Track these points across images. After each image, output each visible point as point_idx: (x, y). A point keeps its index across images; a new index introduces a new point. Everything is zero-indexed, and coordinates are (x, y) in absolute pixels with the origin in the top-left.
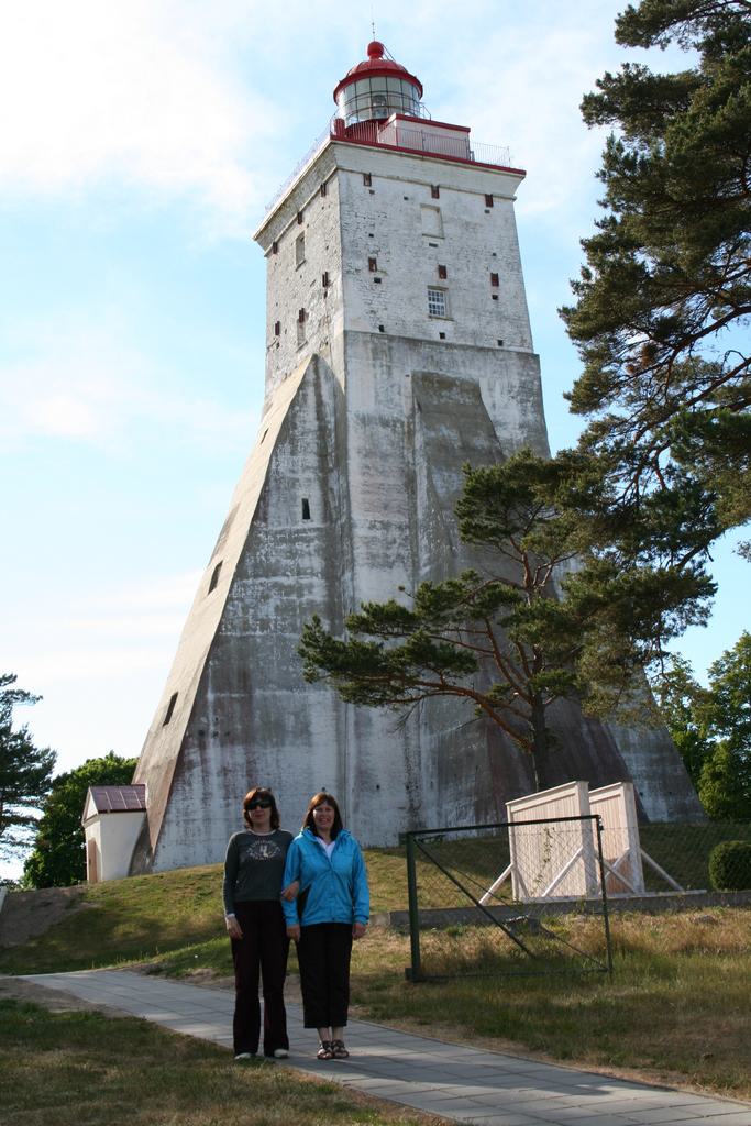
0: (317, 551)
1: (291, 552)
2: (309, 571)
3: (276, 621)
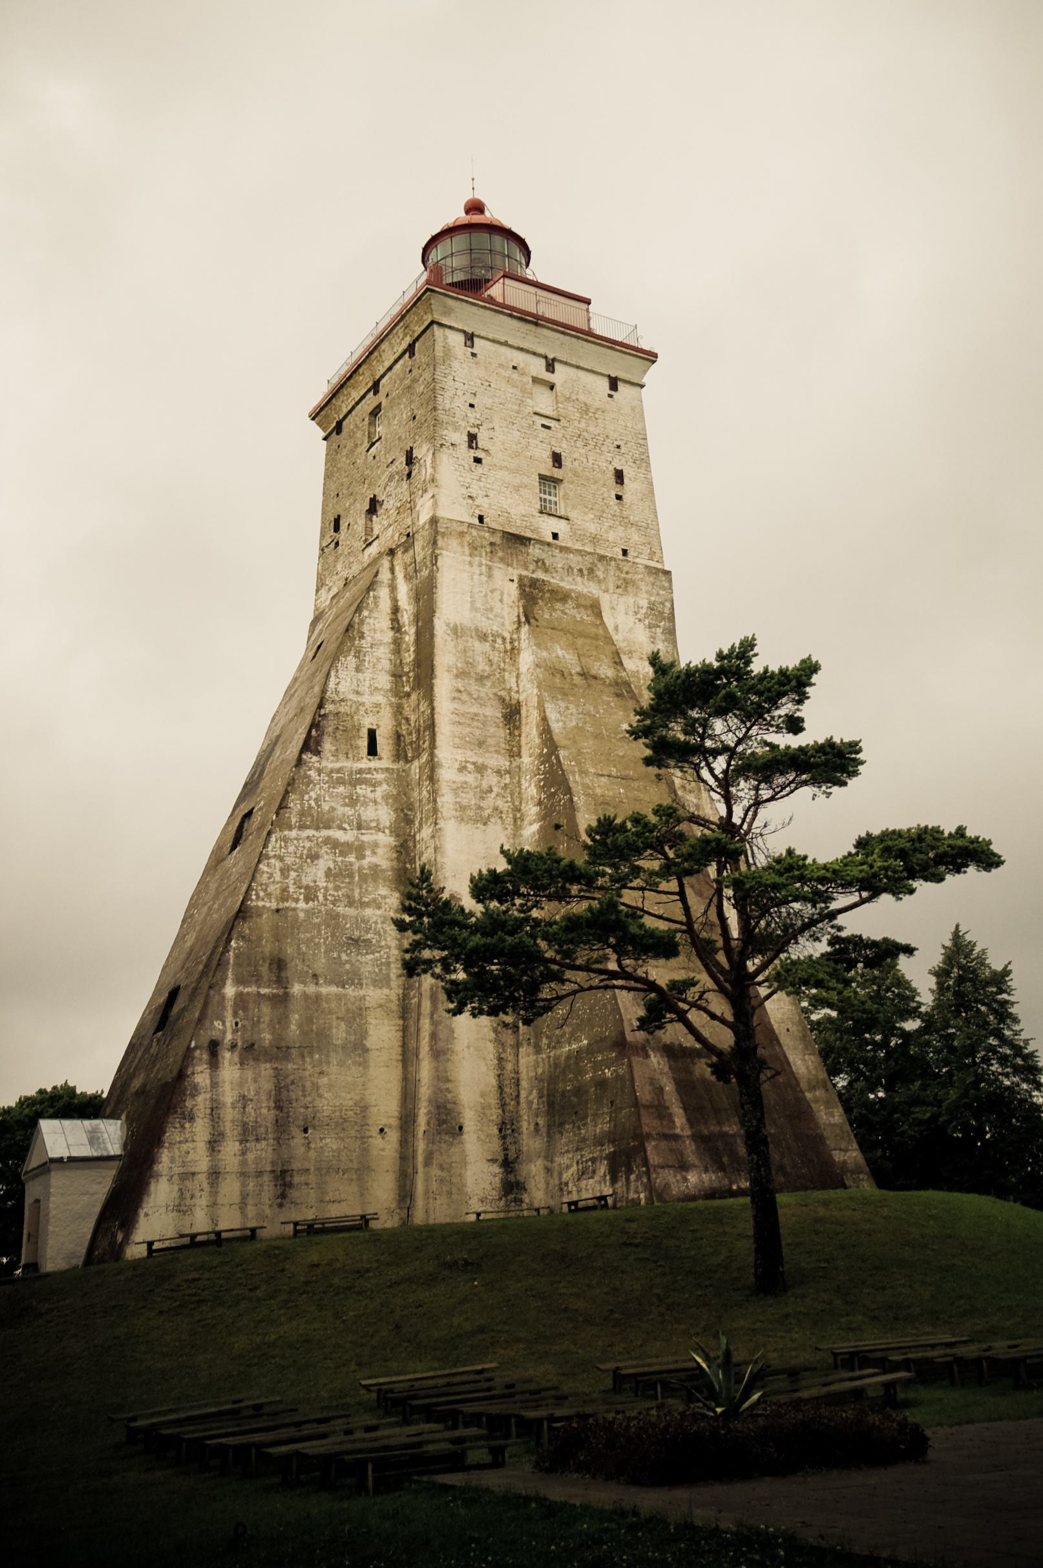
0: (386, 797)
1: (351, 797)
2: (373, 824)
3: (326, 889)
